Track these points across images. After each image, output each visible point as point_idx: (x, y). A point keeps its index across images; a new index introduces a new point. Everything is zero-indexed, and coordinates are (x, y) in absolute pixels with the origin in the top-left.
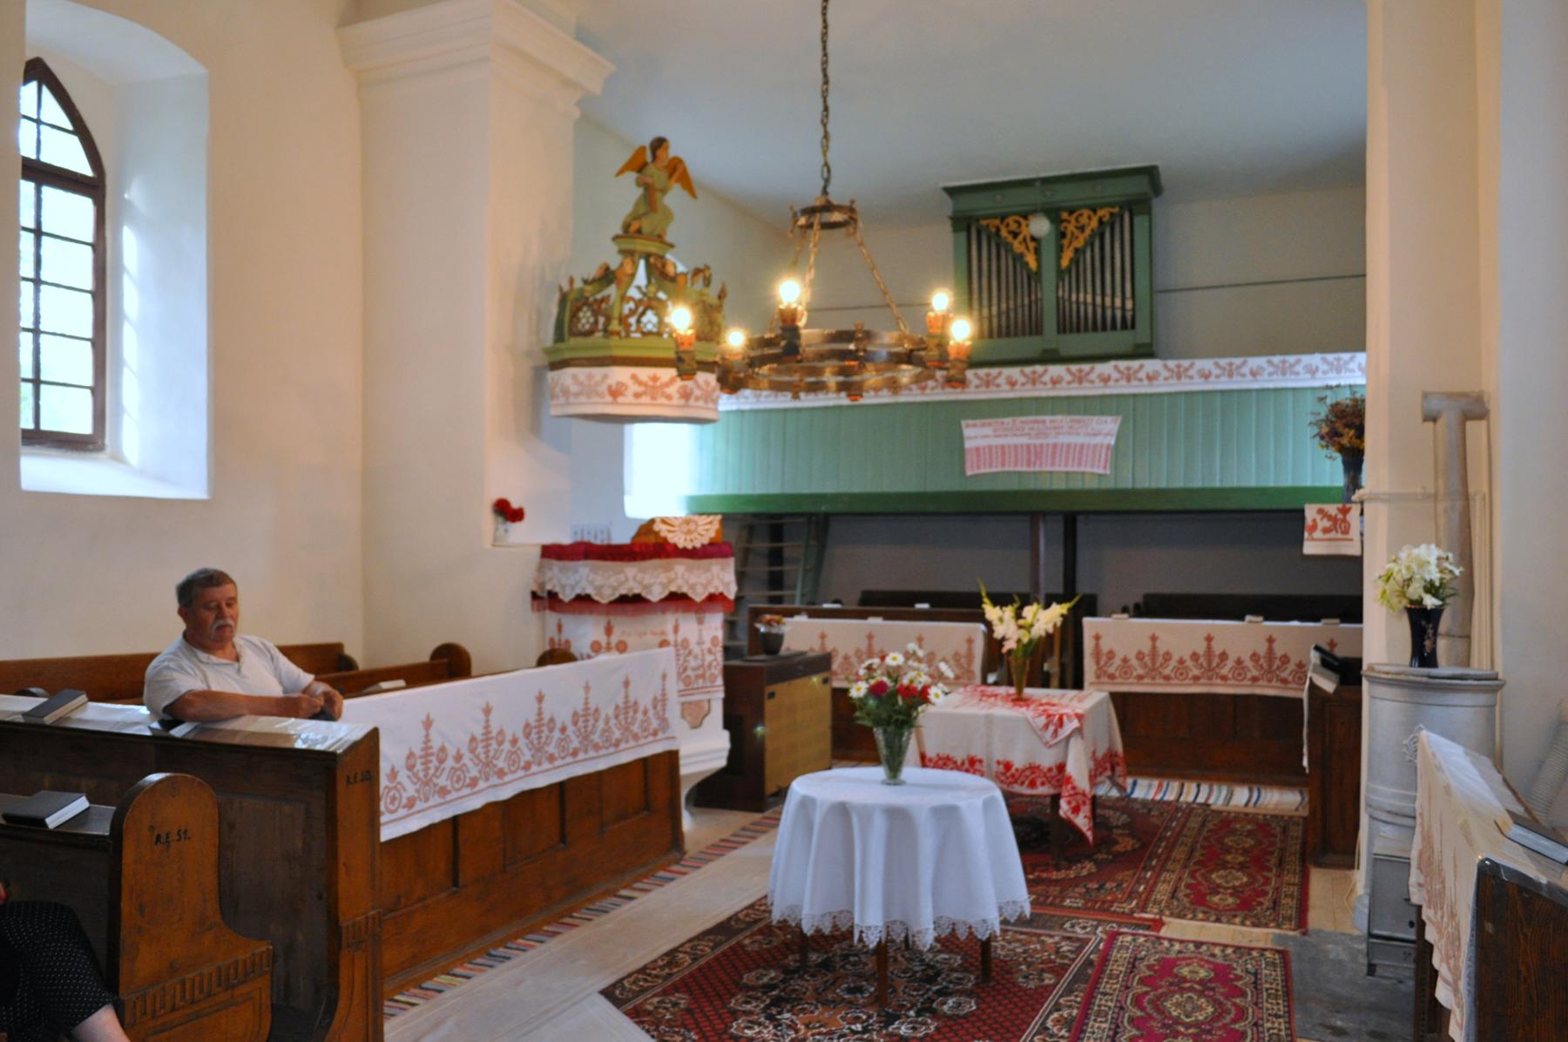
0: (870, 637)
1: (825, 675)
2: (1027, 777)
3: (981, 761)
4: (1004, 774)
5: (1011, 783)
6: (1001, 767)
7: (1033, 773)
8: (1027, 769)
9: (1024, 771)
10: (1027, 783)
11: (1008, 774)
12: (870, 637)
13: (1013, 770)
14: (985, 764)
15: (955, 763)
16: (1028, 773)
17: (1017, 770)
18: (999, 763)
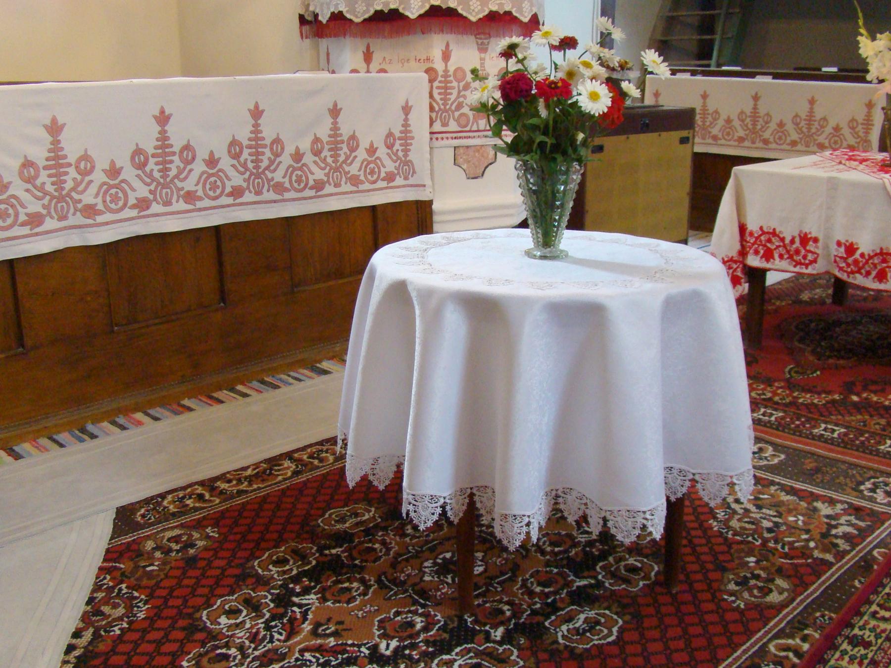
0: (756, 98)
1: (684, 133)
2: (875, 265)
3: (816, 240)
4: (844, 259)
5: (852, 272)
6: (842, 249)
7: (884, 261)
8: (876, 255)
9: (871, 257)
10: (874, 273)
11: (850, 260)
12: (756, 98)
13: (857, 255)
14: (820, 244)
15: (782, 240)
16: (876, 261)
17: (862, 255)
18: (839, 244)
